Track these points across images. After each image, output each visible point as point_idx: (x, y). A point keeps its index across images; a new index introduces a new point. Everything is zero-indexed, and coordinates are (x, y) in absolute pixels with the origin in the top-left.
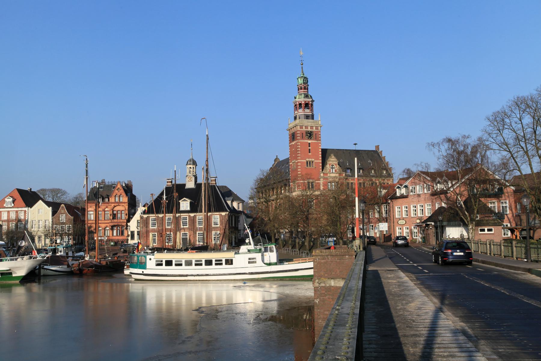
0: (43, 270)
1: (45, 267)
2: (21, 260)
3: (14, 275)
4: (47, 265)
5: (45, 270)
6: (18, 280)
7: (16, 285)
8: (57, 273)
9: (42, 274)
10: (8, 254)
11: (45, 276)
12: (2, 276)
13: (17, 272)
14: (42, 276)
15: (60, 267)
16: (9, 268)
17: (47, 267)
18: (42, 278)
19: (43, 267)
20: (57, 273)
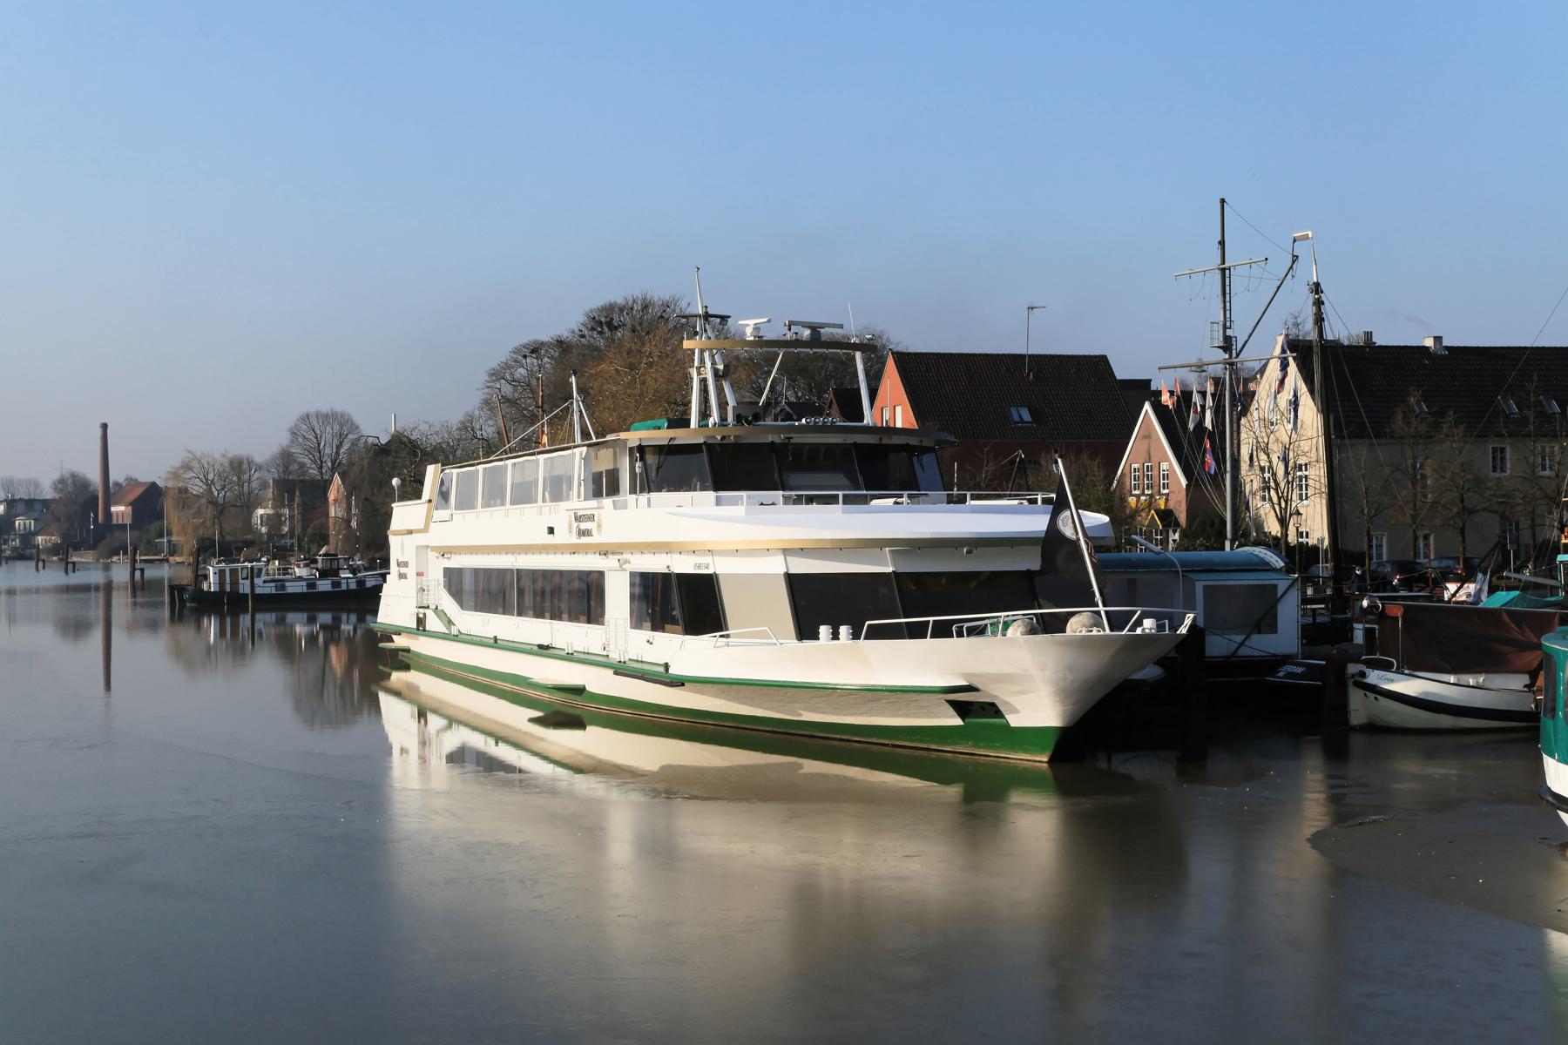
0: (1362, 692)
1: (1375, 677)
2: (1018, 634)
3: (1014, 721)
4: (1387, 667)
5: (1371, 696)
6: (1042, 750)
7: (1024, 779)
8: (1446, 721)
9: (1356, 718)
10: (1292, 585)
11: (1374, 729)
12: (968, 720)
13: (1015, 701)
14: (1354, 729)
15: (1471, 682)
16: (965, 676)
17: (1380, 678)
18: (1357, 742)
19: (1363, 675)
20: (1446, 721)
